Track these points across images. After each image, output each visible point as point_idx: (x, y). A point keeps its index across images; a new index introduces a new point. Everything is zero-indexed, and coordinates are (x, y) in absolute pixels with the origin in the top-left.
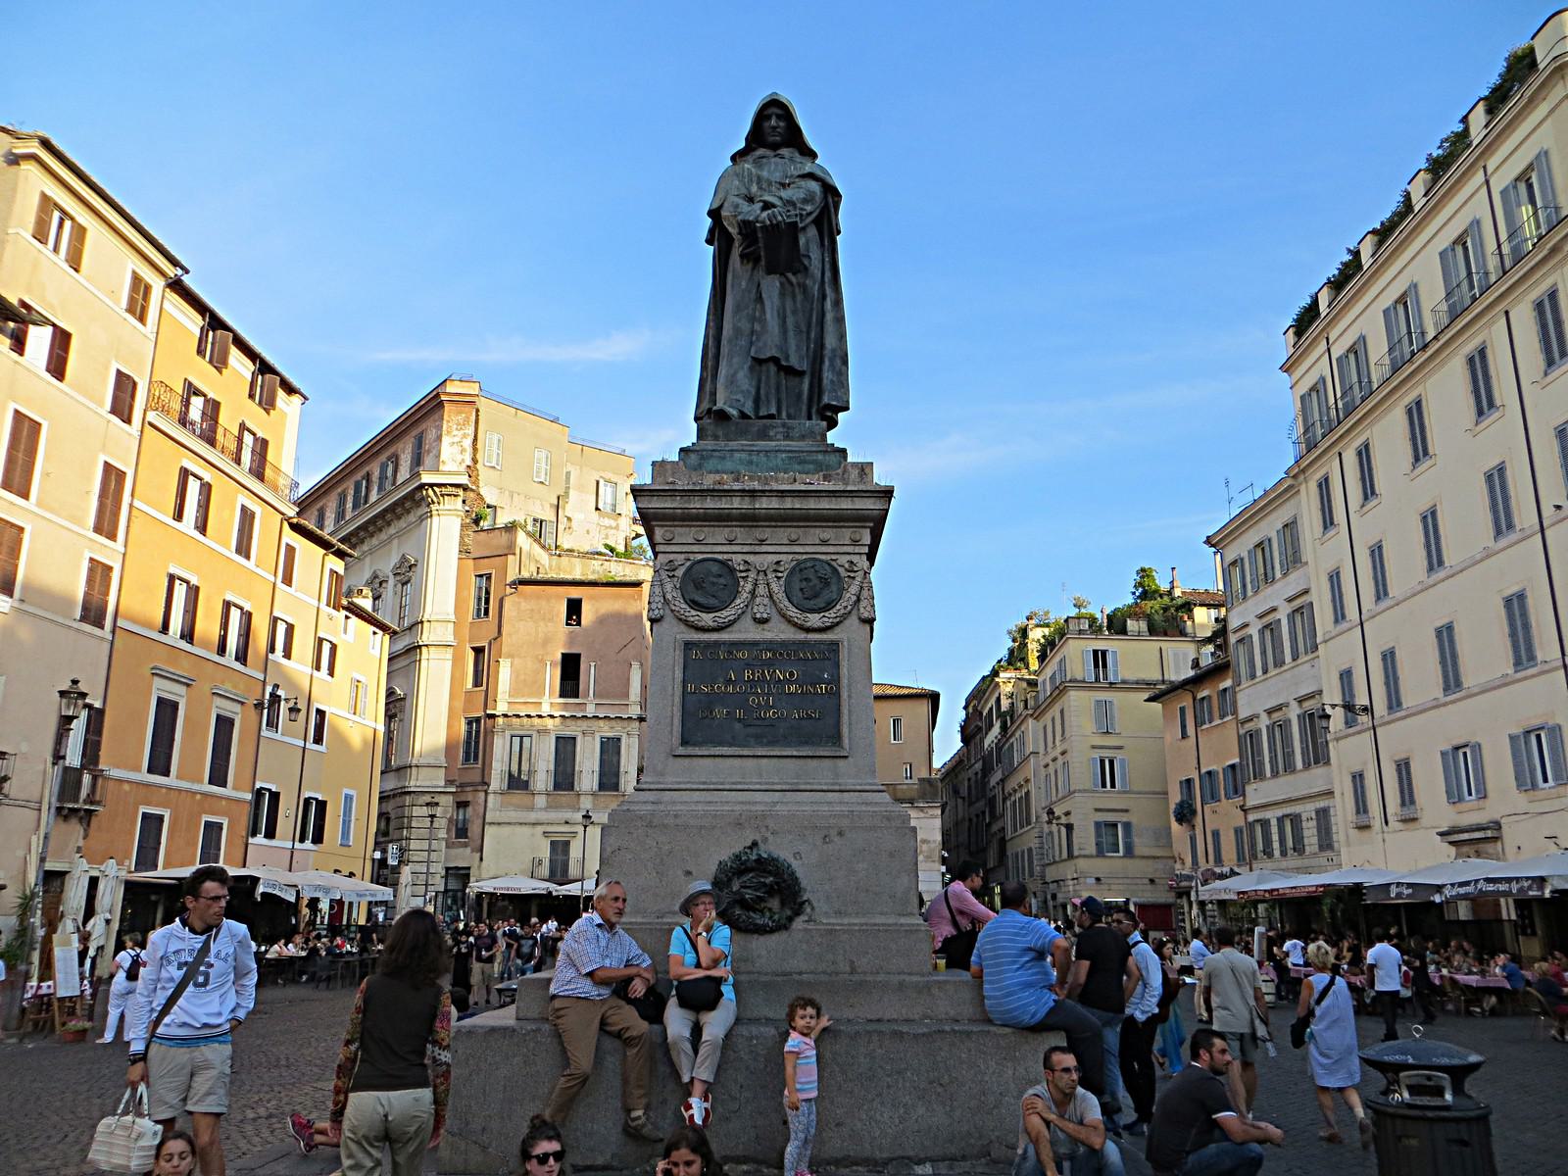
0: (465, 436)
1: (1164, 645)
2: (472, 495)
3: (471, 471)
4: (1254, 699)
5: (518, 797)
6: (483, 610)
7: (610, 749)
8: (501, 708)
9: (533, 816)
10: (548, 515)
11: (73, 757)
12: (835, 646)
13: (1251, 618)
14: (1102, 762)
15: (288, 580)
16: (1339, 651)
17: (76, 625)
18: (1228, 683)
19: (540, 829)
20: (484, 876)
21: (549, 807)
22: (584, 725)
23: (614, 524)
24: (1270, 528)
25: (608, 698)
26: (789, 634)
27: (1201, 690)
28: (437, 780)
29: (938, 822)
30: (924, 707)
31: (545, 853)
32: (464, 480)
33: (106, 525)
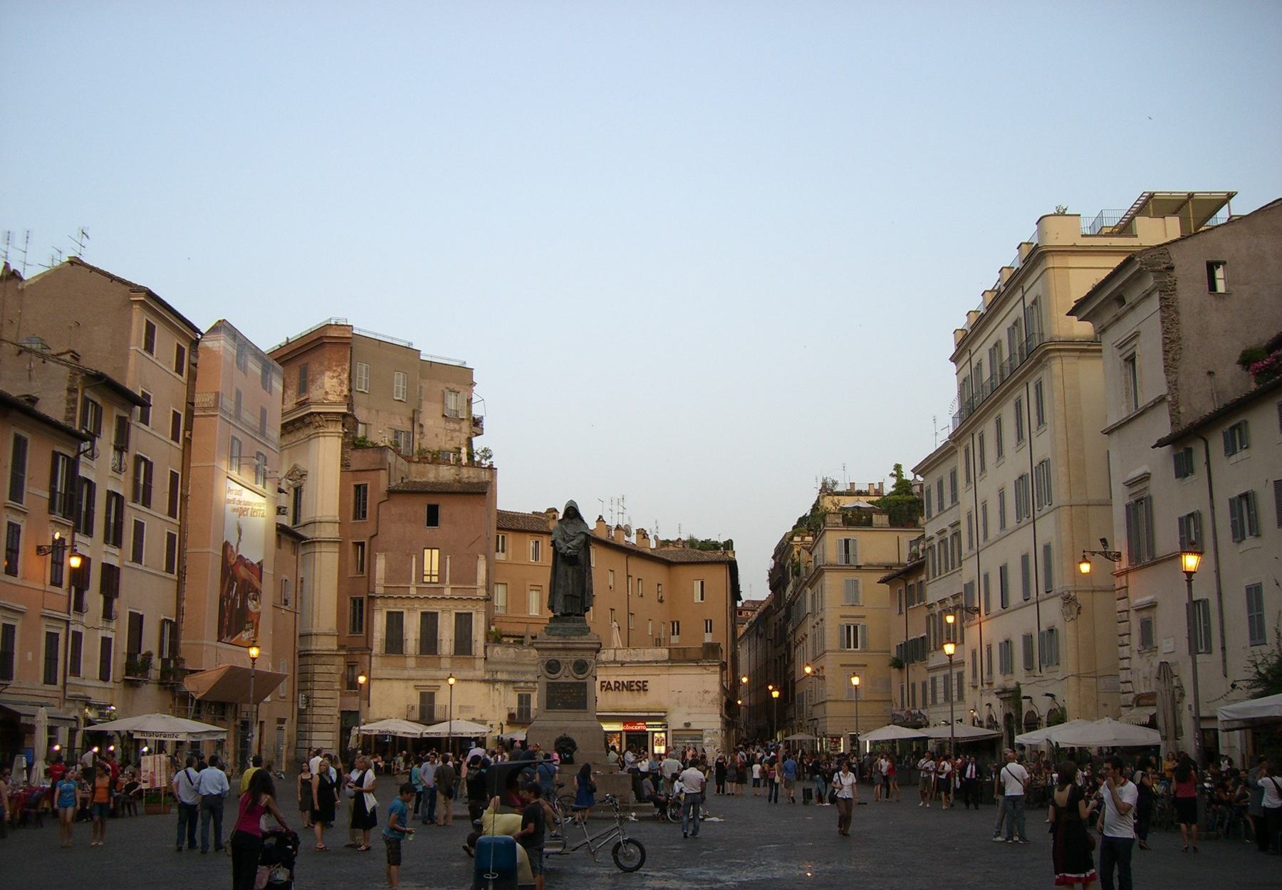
0: (343, 370)
1: (902, 535)
2: (349, 419)
3: (349, 400)
4: (937, 590)
5: (394, 659)
6: (360, 511)
7: (463, 622)
8: (379, 590)
9: (406, 674)
10: (406, 426)
11: (166, 656)
12: (585, 684)
13: (945, 526)
14: (849, 628)
16: (968, 572)
18: (923, 577)
19: (412, 683)
20: (371, 717)
21: (419, 666)
22: (443, 604)
23: (457, 427)
24: (943, 472)
25: (460, 583)
26: (574, 680)
27: (905, 578)
28: (330, 644)
29: (717, 677)
30: (721, 574)
31: (415, 700)
32: (344, 410)
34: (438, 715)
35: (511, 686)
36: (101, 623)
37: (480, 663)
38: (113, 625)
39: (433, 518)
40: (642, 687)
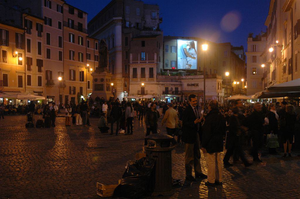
12: (103, 84)
15: (88, 47)
17: (58, 61)
23: (155, 21)
26: (101, 83)
33: (60, 46)
34: (145, 93)
35: (163, 85)
36: (37, 73)
37: (155, 79)
38: (42, 73)
39: (143, 44)
40: (197, 85)
